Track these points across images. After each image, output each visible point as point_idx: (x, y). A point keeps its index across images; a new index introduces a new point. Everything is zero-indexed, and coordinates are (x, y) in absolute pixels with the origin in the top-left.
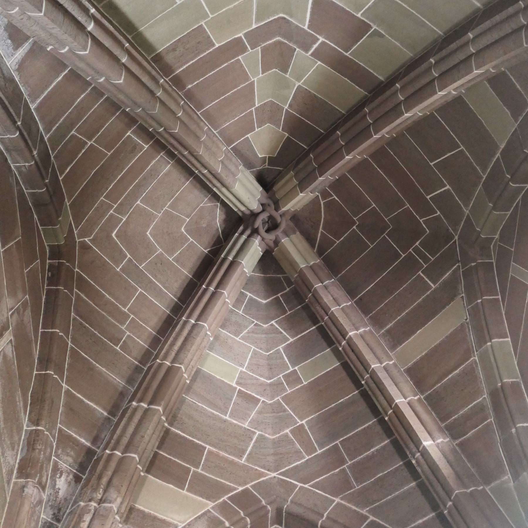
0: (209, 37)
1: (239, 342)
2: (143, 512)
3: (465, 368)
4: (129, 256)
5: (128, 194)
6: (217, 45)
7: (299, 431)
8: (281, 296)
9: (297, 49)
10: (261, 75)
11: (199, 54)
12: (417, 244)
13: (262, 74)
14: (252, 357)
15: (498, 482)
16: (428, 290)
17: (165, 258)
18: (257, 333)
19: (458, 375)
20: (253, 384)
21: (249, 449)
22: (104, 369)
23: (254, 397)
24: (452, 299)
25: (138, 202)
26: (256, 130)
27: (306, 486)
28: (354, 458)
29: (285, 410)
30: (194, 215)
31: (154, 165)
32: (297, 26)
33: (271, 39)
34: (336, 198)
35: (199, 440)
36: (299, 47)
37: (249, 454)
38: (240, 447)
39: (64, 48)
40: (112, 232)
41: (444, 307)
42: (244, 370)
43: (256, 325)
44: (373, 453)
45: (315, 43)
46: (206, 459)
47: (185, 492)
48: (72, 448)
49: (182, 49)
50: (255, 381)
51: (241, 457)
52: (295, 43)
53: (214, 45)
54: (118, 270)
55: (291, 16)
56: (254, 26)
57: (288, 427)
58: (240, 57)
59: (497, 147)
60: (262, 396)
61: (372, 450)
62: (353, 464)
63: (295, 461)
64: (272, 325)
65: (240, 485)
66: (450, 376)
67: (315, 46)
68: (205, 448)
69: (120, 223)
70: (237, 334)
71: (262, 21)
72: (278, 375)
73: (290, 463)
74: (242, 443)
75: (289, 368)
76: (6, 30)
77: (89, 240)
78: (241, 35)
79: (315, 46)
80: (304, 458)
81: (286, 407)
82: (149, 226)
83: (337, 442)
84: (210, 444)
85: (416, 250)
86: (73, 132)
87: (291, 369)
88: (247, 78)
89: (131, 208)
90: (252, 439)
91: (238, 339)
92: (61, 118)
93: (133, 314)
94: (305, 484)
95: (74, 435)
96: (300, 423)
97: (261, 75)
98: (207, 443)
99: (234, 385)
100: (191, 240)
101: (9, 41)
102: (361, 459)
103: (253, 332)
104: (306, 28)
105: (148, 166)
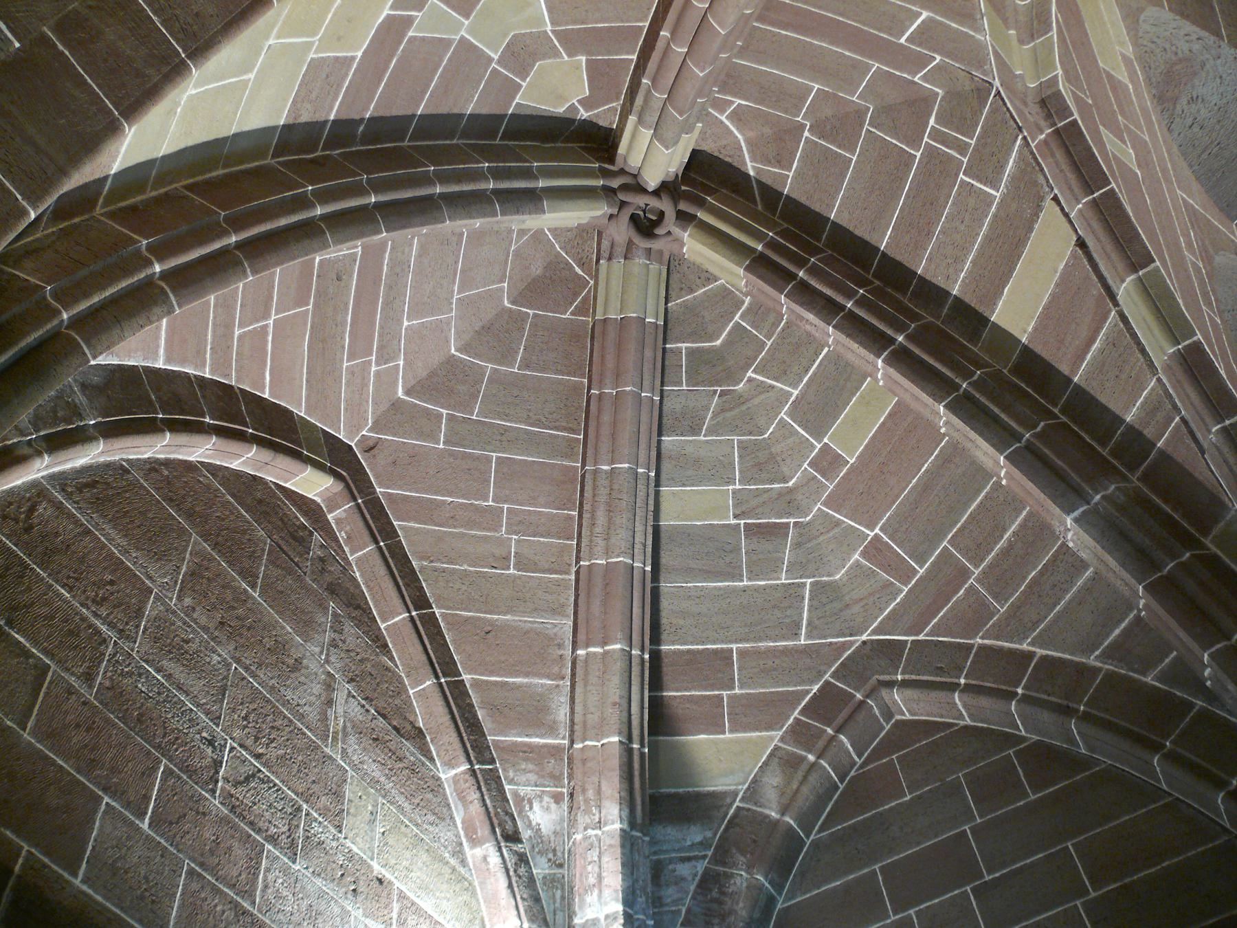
0: (337, 58)
1: (707, 442)
2: (676, 795)
3: (1106, 334)
4: (445, 412)
7: (875, 550)
8: (742, 317)
10: (467, 23)
11: (340, 86)
12: (932, 121)
14: (740, 457)
15: (1222, 524)
16: (990, 206)
18: (731, 409)
19: (1101, 351)
21: (805, 616)
22: (508, 617)
24: (1039, 208)
26: (524, 84)
27: (921, 637)
28: (982, 560)
29: (838, 523)
35: (714, 643)
37: (809, 624)
38: (788, 620)
40: (396, 393)
41: (1031, 229)
42: (738, 487)
43: (723, 393)
44: (1009, 540)
46: (739, 670)
47: (728, 735)
48: (526, 760)
50: (765, 496)
51: (796, 635)
54: (441, 446)
57: (855, 550)
60: (790, 515)
61: (1006, 537)
62: (984, 572)
63: (888, 603)
64: (750, 380)
65: (812, 682)
66: (1089, 357)
70: (695, 430)
72: (800, 466)
73: (882, 610)
74: (788, 613)
75: (813, 447)
77: (369, 431)
80: (901, 591)
82: (448, 342)
84: (736, 642)
85: (935, 135)
90: (803, 598)
91: (702, 438)
93: (505, 502)
94: (917, 635)
95: (519, 739)
98: (731, 642)
99: (733, 522)
103: (723, 411)
105: (382, 270)
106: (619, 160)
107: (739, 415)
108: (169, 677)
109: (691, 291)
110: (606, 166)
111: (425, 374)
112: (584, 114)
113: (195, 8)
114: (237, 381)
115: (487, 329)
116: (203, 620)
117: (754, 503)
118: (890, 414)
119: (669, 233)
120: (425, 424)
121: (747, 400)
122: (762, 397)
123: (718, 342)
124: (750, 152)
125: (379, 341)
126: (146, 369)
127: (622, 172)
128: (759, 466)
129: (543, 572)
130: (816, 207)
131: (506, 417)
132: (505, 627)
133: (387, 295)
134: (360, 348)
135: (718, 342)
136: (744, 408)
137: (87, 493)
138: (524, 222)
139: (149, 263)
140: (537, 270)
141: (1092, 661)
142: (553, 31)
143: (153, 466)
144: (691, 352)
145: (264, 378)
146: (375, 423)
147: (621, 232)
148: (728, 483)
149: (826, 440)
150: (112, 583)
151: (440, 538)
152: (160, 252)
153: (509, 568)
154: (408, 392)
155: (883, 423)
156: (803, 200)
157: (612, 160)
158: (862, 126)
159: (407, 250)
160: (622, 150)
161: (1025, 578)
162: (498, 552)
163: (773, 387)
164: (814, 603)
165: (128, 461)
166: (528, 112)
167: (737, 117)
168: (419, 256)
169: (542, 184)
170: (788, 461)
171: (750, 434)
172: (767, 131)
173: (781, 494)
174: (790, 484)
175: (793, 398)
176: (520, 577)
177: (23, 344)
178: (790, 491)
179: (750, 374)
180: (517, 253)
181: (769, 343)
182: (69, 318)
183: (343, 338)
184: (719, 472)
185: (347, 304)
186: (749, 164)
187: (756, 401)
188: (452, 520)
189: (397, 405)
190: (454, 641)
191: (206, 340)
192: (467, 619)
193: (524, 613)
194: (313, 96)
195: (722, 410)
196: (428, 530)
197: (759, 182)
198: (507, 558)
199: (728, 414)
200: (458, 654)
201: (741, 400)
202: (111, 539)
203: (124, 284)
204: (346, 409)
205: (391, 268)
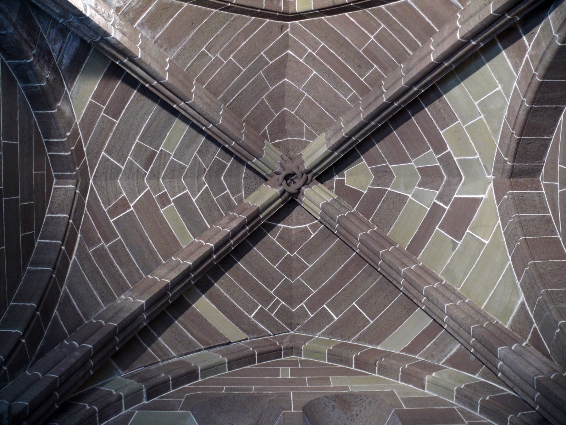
0: (448, 126)
2: (83, 62)
3: (193, 341)
4: (271, 63)
5: (323, 64)
6: (441, 132)
7: (124, 205)
8: (227, 193)
9: (438, 192)
10: (416, 167)
11: (436, 119)
12: (283, 303)
13: (417, 168)
14: (181, 165)
15: (116, 366)
16: (247, 312)
17: (265, 93)
18: (198, 170)
19: (187, 337)
20: (160, 165)
21: (112, 160)
23: (150, 166)
24: (244, 331)
25: (315, 72)
26: (369, 168)
29: (140, 193)
30: (297, 119)
31: (346, 85)
32: (456, 190)
33: (445, 172)
34: (312, 237)
35: (124, 114)
36: (439, 193)
37: (108, 159)
38: (114, 151)
39: (460, 24)
41: (237, 325)
42: (171, 157)
44: (116, 267)
45: (444, 204)
46: (109, 119)
47: (90, 99)
48: (141, 6)
49: (440, 107)
50: (162, 167)
51: (106, 151)
52: (443, 190)
53: (442, 130)
54: (262, 53)
55: (463, 184)
56: (455, 159)
57: (127, 195)
58: (431, 150)
59: (378, 344)
60: (150, 173)
61: (118, 266)
63: (102, 199)
64: (204, 184)
65: (87, 149)
66: (185, 330)
67: (441, 204)
68: (117, 120)
69: (298, 57)
70: (200, 152)
71: (460, 164)
73: (100, 195)
74: (116, 153)
75: (172, 197)
78: (449, 149)
79: (441, 204)
80: (106, 208)
81: (143, 194)
82: (292, 80)
83: (120, 237)
84: (119, 124)
85: (277, 302)
86: (383, 25)
87: (171, 200)
88: (413, 157)
89: (310, 66)
90: (118, 162)
91: (195, 153)
92: (396, 18)
93: (227, 64)
95: (149, 9)
96: (131, 206)
97: (416, 167)
98: (120, 121)
100: (276, 115)
102: (110, 257)
103: (200, 167)
104: (455, 196)
105: (345, 80)
106: (316, 182)
107: (196, 172)
109: (245, 178)
110: (317, 176)
111: (288, 65)
112: (336, 178)
114: (365, 11)
115: (283, 96)
117: (162, 161)
118: (174, 236)
119: (282, 185)
120: (271, 54)
121: (198, 179)
122: (197, 185)
123: (222, 178)
124: (287, 228)
125: (318, 60)
128: (173, 171)
129: (194, 61)
130: (260, 243)
131: (252, 83)
132: (188, 33)
133: (333, 74)
134: (323, 53)
135: (222, 178)
136: (196, 176)
140: (288, 127)
141: (65, 287)
142: (387, 190)
144: (225, 166)
145: (354, 18)
146: (288, 35)
148: (175, 154)
149: (172, 204)
151: (236, 30)
153: (206, 48)
154: (287, 54)
155: (172, 231)
156: (264, 240)
157: (317, 179)
158: (286, 275)
159: (343, 92)
160: (320, 184)
161: (101, 268)
162: (214, 48)
163: (199, 192)
164: (114, 166)
166: (355, 162)
167: (305, 230)
168: (336, 94)
170: (170, 183)
171: (186, 173)
172: (293, 239)
173: (159, 174)
174: (161, 180)
175: (192, 198)
176: (199, 51)
178: (158, 178)
179: (207, 185)
181: (215, 199)
183: (334, 51)
184: (180, 154)
185: (346, 62)
186: (283, 226)
187: (196, 182)
188: (237, 39)
189: (287, 47)
190: (201, 9)
191: (395, 16)
192: (203, 20)
193: (187, 43)
194: (442, 111)
195: (200, 166)
196: (241, 28)
197: (275, 226)
198: (209, 51)
199: (197, 168)
200: (196, 7)
201: (199, 176)
204: (305, 31)
205: (342, 83)
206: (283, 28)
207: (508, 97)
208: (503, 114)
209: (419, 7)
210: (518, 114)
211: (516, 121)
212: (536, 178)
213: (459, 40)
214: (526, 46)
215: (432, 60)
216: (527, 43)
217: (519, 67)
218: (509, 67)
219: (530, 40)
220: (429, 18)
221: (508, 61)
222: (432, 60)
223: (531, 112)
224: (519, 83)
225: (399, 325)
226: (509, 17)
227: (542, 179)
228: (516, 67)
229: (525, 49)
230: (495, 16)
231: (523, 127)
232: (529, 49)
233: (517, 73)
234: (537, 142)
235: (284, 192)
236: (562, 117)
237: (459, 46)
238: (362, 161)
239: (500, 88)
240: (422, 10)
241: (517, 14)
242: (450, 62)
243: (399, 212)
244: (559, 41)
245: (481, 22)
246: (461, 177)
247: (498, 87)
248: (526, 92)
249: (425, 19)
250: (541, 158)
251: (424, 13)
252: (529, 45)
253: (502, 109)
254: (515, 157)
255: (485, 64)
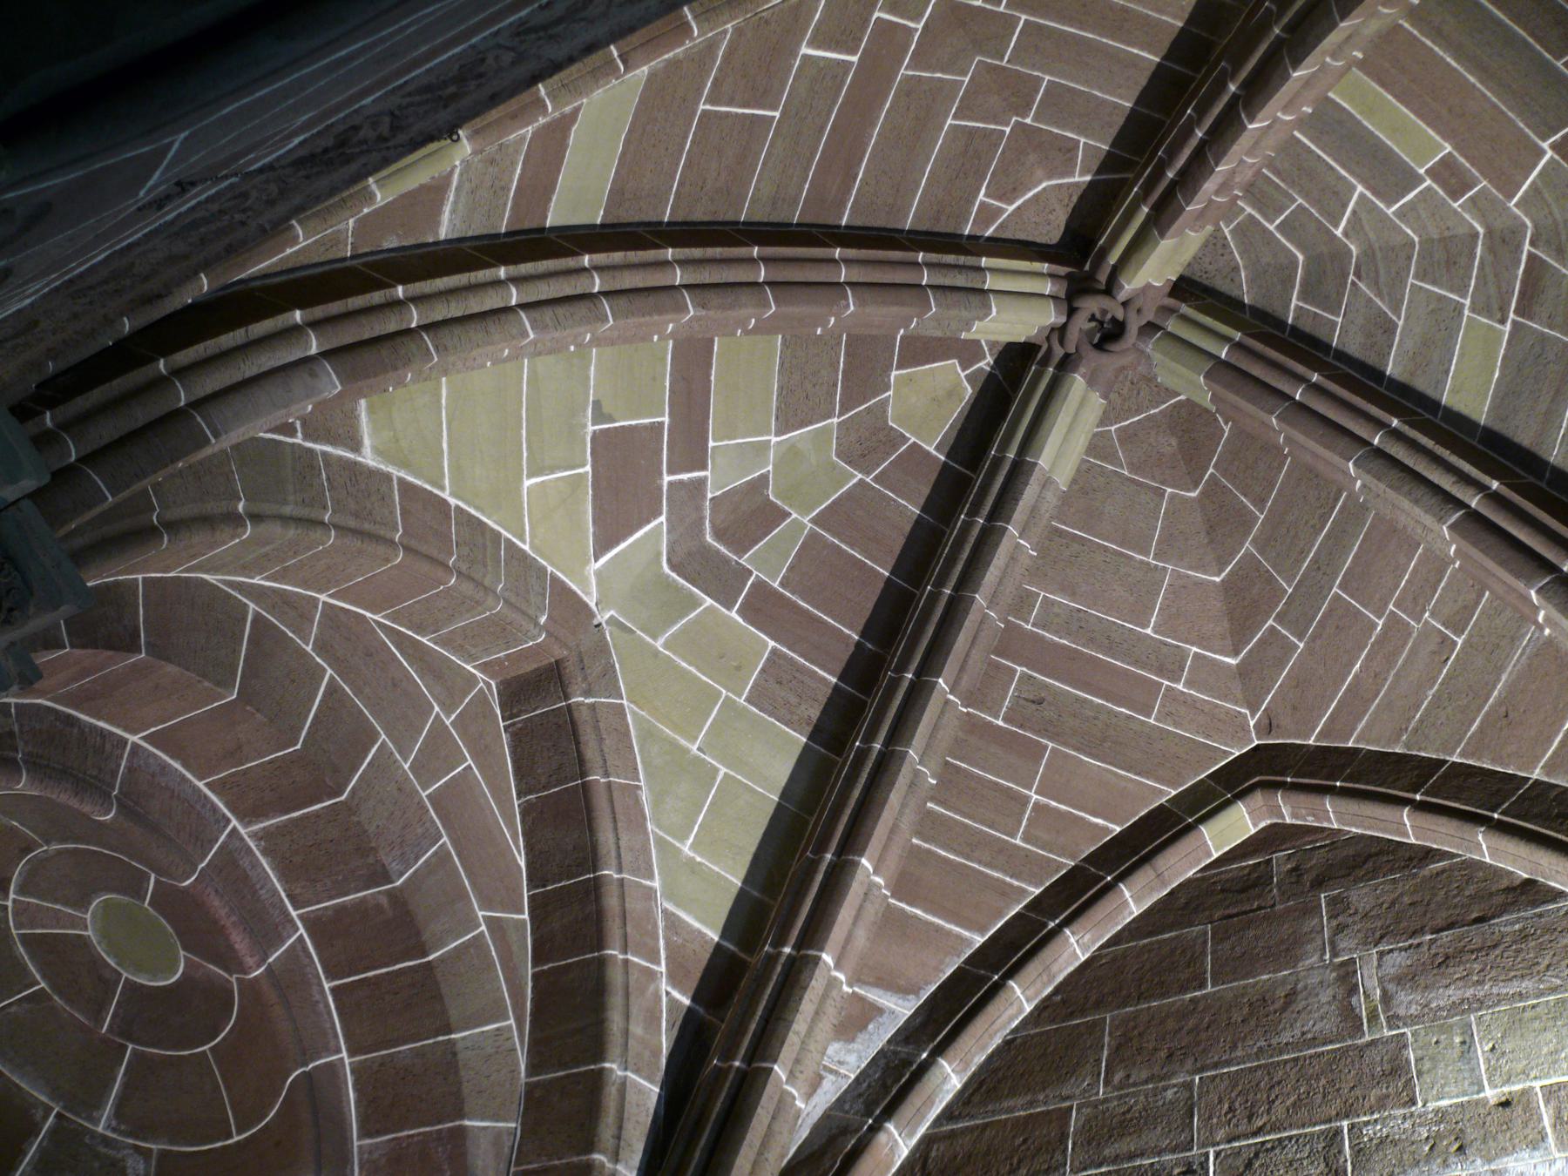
1: (1407, 319)
4: (1270, 622)
5: (1136, 663)
6: (772, 643)
8: (1271, 222)
9: (710, 496)
10: (794, 515)
14: (1434, 283)
17: (1261, 531)
18: (1377, 272)
20: (1496, 276)
22: (1504, 678)
23: (1525, 271)
25: (1149, 631)
26: (913, 439)
30: (1153, 478)
31: (1056, 633)
32: (669, 532)
33: (718, 551)
36: (705, 496)
39: (836, 979)
40: (1229, 665)
42: (1468, 302)
43: (1358, 274)
45: (681, 482)
49: (803, 707)
50: (1488, 269)
52: (699, 509)
53: (774, 651)
55: (659, 554)
56: (709, 601)
58: (776, 585)
59: (652, 76)
60: (1518, 248)
64: (1346, 233)
67: (685, 476)
69: (1205, 657)
70: (1390, 329)
71: (691, 594)
72: (1455, 211)
75: (1429, 189)
76: (853, 1040)
77: (1253, 716)
78: (734, 614)
79: (685, 476)
81: (1525, 187)
82: (1200, 584)
86: (1018, 842)
87: (1428, 182)
88: (813, 536)
89: (1165, 644)
91: (1401, 323)
92: (992, 878)
93: (1386, 605)
96: (1550, 153)
97: (794, 515)
99: (1508, 327)
100: (1211, 470)
101: (871, 1027)
103: (1377, 283)
104: (663, 518)
107: (1385, 262)
108: (1116, 1159)
109: (1236, 269)
110: (1040, 355)
111: (1226, 624)
113: (570, 847)
114: (1073, 857)
115: (1211, 529)
116: (1144, 1075)
117: (1492, 290)
118: (1383, 85)
119: (1125, 304)
120: (1275, 648)
121: (1371, 246)
122: (1367, 228)
123: (1301, 257)
124: (1062, 175)
125: (1150, 671)
126: (969, 961)
127: (1048, 338)
128: (1450, 263)
129: (1477, 603)
130: (1121, 121)
131: (1303, 553)
132: (1511, 688)
133: (1099, 648)
134: (1142, 695)
136: (1379, 255)
137: (976, 1099)
138: (1047, 483)
139: (780, 953)
140: (1169, 444)
143: (1044, 1010)
144: (1304, 296)
145: (1097, 825)
146: (1248, 707)
147: (1109, 363)
148: (1461, 314)
149: (1422, 171)
150: (1025, 1141)
151: (1387, 705)
152: (780, 942)
153: (1455, 643)
154: (1236, 653)
155: (1395, 96)
156: (1114, 131)
158: (1004, 68)
159: (1056, 610)
162: (1433, 647)
163: (1354, 212)
165: (1012, 1032)
168: (1073, 595)
169: (1011, 455)
170: (1450, 224)
171: (1410, 258)
172: (1032, 157)
173: (1490, 249)
174: (1481, 230)
175: (1368, 194)
176: (1470, 636)
177: (714, 1116)
178: (1490, 233)
179: (1339, 232)
180: (1133, 468)
181: (1300, 201)
182: (743, 1061)
184: (1447, 316)
185: (1078, 699)
186: (1077, 179)
187: (1372, 236)
188: (1379, 678)
189: (1243, 671)
190: (1493, 761)
191: (998, 879)
192: (1480, 728)
193: (1508, 656)
194: (794, 700)
195: (1375, 284)
196: (1375, 712)
197: (1098, 172)
198: (1445, 638)
199: (1382, 279)
200: (1507, 766)
201: (1368, 254)
202: (1017, 1108)
203: (769, 991)
204: (1208, 737)
205: (1068, 634)
206: (1267, 727)
207: (660, 842)
208: (650, 789)
209: (949, 933)
210: (616, 829)
211: (613, 812)
212: (502, 683)
213: (822, 950)
214: (674, 986)
215: (864, 861)
216: (676, 994)
217: (666, 927)
218: (689, 912)
219: (673, 1002)
220: (915, 917)
221: (697, 925)
222: (864, 861)
223: (589, 857)
224: (650, 893)
225: (623, 153)
226: (737, 1064)
227: (489, 685)
228: (673, 923)
229: (674, 979)
230: (765, 1060)
231: (589, 809)
232: (664, 986)
233: (665, 911)
234: (543, 780)
235: (1109, 290)
236: (522, 863)
237: (815, 933)
238: (937, 448)
239: (686, 848)
240: (939, 929)
241: (720, 1074)
242: (823, 867)
243: (781, 388)
244: (611, 1070)
245: (788, 1028)
246: (673, 567)
247: (692, 847)
248: (622, 897)
249: (925, 911)
250: (520, 738)
251: (932, 924)
252: (668, 993)
253: (657, 803)
254: (573, 723)
255: (745, 881)
